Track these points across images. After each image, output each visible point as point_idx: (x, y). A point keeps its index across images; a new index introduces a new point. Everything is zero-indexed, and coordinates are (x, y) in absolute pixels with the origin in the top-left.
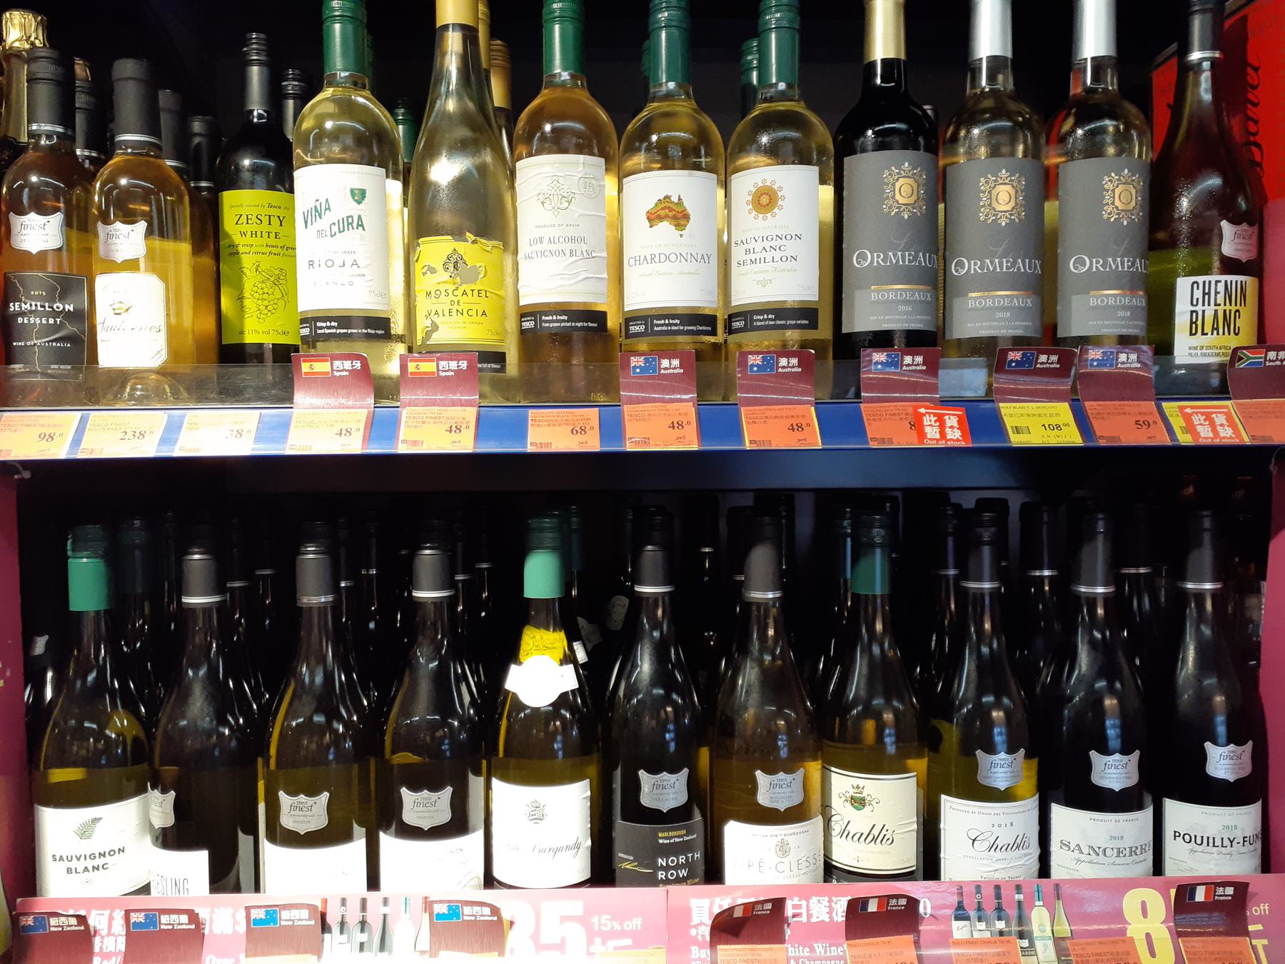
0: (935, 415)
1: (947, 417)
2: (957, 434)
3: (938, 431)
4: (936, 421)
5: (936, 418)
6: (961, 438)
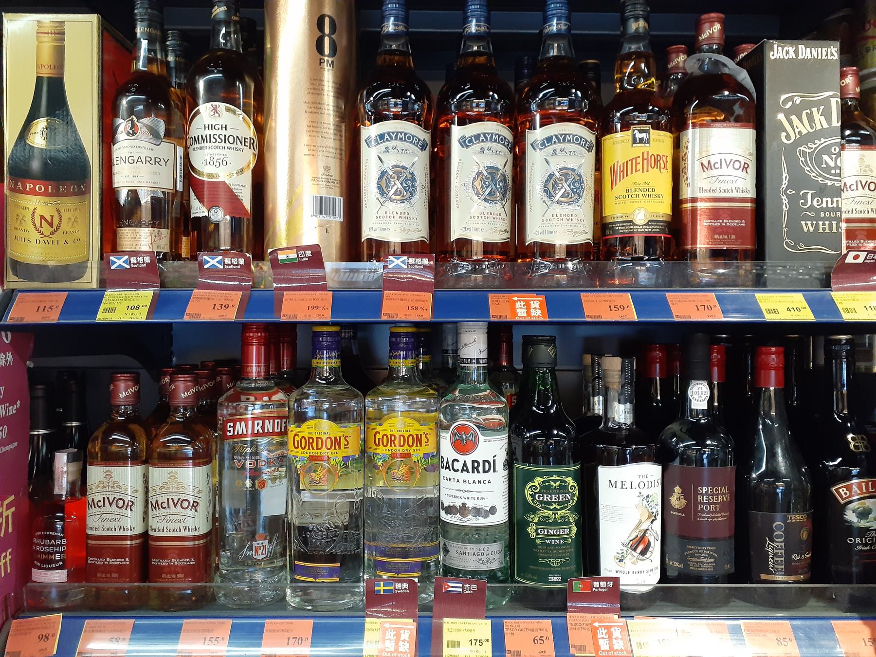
0: (524, 301)
1: (532, 302)
2: (539, 312)
3: (525, 311)
4: (524, 305)
5: (524, 303)
6: (541, 315)
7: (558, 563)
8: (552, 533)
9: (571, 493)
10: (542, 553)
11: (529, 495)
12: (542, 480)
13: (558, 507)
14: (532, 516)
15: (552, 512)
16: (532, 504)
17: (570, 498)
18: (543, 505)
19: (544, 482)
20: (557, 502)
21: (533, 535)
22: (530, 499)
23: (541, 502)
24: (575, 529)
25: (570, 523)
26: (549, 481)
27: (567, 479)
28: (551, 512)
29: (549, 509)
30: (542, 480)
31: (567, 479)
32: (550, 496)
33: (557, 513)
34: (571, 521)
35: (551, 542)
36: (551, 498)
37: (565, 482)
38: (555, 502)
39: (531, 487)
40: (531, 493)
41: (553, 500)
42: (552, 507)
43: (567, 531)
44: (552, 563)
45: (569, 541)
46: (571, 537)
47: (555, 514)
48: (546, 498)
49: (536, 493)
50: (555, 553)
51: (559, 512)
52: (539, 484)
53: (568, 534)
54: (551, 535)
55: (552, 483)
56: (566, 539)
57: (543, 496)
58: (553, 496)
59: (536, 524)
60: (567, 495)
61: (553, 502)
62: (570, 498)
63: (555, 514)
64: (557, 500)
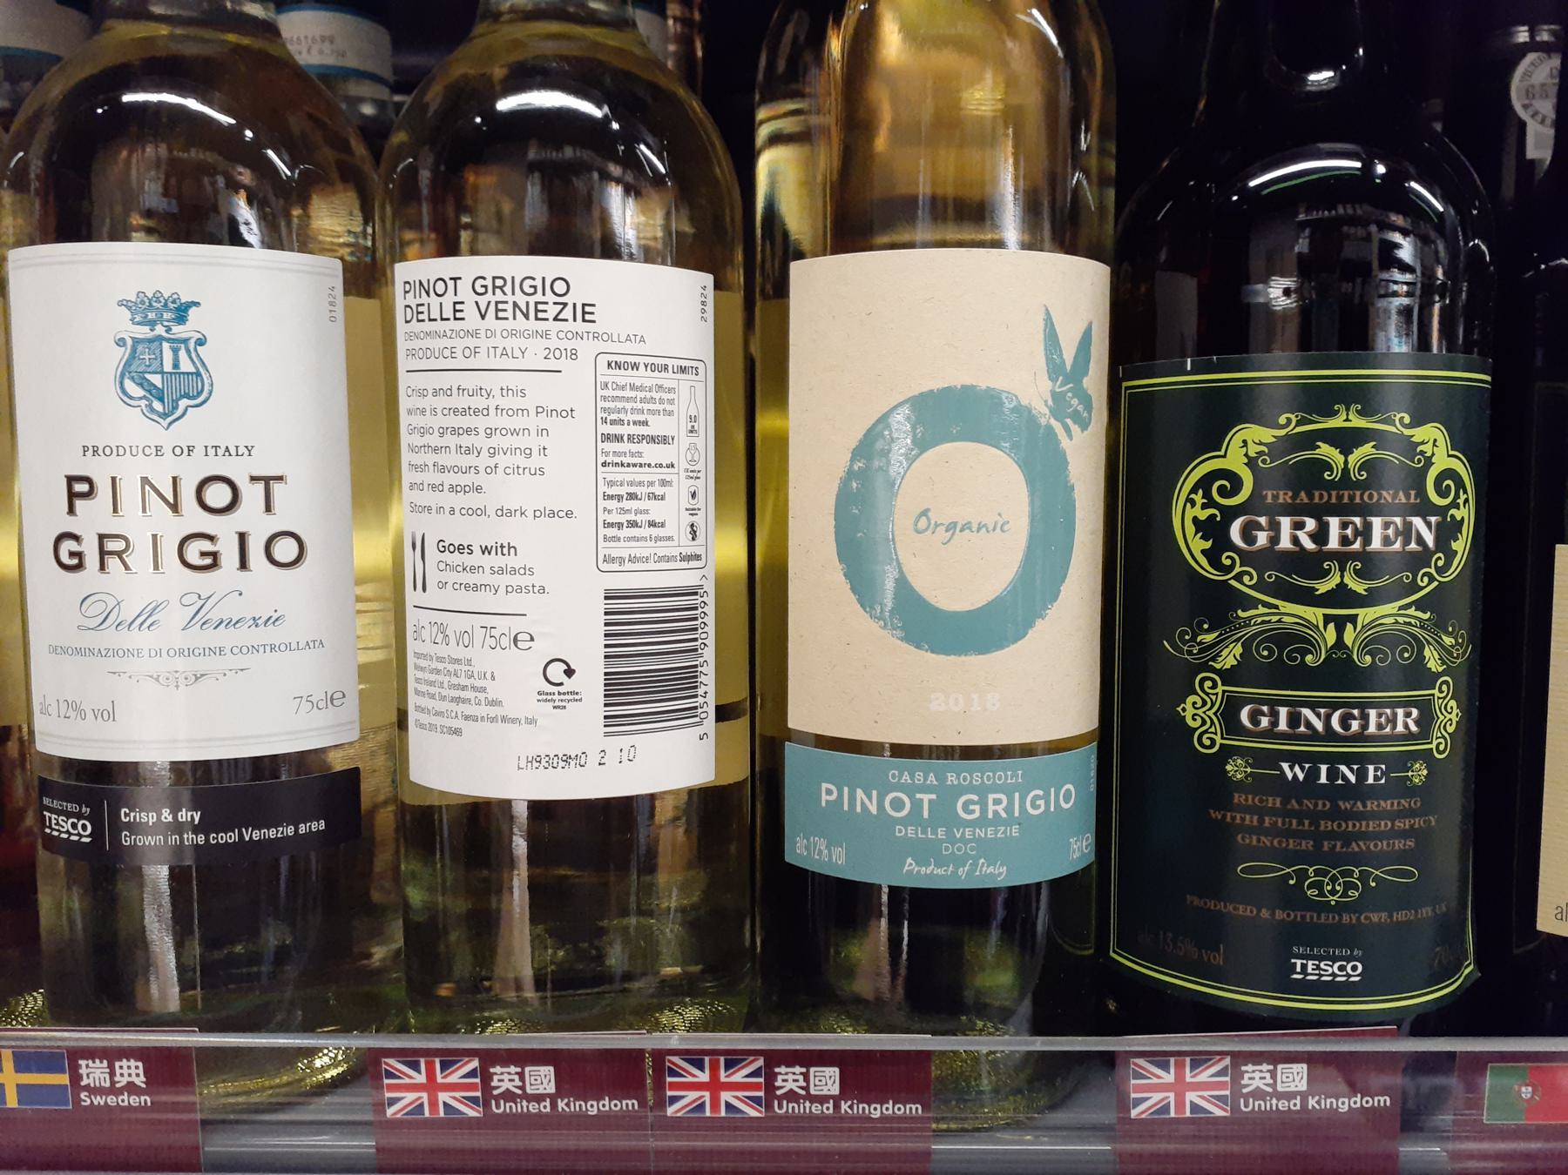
7: (1349, 886)
8: (1319, 726)
9: (1442, 510)
10: (1259, 830)
11: (1190, 528)
12: (1267, 435)
13: (1359, 587)
14: (1209, 638)
15: (1320, 612)
16: (1213, 574)
17: (1429, 539)
18: (1271, 576)
19: (1275, 449)
20: (1354, 556)
21: (1211, 738)
22: (1195, 546)
23: (1268, 558)
24: (1450, 715)
25: (1430, 679)
26: (1309, 440)
27: (1419, 434)
28: (1315, 614)
29: (1308, 598)
30: (1267, 435)
31: (1419, 434)
32: (1311, 524)
33: (1353, 619)
34: (1434, 664)
35: (1313, 774)
36: (1320, 536)
37: (1411, 448)
38: (1342, 558)
39: (1205, 483)
40: (1203, 515)
41: (1333, 543)
42: (1323, 587)
43: (1406, 721)
44: (1318, 885)
45: (1419, 772)
46: (1427, 756)
47: (1340, 622)
48: (1290, 534)
49: (1230, 514)
50: (1331, 835)
51: (1365, 615)
52: (1251, 463)
53: (1408, 737)
54: (1313, 736)
55: (1325, 450)
56: (1405, 760)
57: (1275, 527)
58: (1334, 523)
59: (1228, 676)
60: (1417, 522)
61: (1333, 555)
62: (1429, 539)
63: (1340, 622)
64: (1357, 546)
